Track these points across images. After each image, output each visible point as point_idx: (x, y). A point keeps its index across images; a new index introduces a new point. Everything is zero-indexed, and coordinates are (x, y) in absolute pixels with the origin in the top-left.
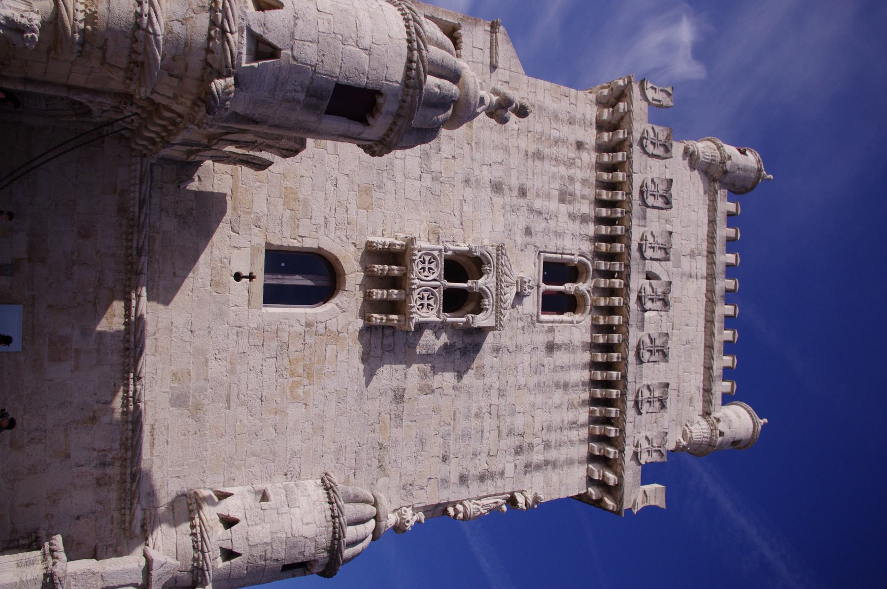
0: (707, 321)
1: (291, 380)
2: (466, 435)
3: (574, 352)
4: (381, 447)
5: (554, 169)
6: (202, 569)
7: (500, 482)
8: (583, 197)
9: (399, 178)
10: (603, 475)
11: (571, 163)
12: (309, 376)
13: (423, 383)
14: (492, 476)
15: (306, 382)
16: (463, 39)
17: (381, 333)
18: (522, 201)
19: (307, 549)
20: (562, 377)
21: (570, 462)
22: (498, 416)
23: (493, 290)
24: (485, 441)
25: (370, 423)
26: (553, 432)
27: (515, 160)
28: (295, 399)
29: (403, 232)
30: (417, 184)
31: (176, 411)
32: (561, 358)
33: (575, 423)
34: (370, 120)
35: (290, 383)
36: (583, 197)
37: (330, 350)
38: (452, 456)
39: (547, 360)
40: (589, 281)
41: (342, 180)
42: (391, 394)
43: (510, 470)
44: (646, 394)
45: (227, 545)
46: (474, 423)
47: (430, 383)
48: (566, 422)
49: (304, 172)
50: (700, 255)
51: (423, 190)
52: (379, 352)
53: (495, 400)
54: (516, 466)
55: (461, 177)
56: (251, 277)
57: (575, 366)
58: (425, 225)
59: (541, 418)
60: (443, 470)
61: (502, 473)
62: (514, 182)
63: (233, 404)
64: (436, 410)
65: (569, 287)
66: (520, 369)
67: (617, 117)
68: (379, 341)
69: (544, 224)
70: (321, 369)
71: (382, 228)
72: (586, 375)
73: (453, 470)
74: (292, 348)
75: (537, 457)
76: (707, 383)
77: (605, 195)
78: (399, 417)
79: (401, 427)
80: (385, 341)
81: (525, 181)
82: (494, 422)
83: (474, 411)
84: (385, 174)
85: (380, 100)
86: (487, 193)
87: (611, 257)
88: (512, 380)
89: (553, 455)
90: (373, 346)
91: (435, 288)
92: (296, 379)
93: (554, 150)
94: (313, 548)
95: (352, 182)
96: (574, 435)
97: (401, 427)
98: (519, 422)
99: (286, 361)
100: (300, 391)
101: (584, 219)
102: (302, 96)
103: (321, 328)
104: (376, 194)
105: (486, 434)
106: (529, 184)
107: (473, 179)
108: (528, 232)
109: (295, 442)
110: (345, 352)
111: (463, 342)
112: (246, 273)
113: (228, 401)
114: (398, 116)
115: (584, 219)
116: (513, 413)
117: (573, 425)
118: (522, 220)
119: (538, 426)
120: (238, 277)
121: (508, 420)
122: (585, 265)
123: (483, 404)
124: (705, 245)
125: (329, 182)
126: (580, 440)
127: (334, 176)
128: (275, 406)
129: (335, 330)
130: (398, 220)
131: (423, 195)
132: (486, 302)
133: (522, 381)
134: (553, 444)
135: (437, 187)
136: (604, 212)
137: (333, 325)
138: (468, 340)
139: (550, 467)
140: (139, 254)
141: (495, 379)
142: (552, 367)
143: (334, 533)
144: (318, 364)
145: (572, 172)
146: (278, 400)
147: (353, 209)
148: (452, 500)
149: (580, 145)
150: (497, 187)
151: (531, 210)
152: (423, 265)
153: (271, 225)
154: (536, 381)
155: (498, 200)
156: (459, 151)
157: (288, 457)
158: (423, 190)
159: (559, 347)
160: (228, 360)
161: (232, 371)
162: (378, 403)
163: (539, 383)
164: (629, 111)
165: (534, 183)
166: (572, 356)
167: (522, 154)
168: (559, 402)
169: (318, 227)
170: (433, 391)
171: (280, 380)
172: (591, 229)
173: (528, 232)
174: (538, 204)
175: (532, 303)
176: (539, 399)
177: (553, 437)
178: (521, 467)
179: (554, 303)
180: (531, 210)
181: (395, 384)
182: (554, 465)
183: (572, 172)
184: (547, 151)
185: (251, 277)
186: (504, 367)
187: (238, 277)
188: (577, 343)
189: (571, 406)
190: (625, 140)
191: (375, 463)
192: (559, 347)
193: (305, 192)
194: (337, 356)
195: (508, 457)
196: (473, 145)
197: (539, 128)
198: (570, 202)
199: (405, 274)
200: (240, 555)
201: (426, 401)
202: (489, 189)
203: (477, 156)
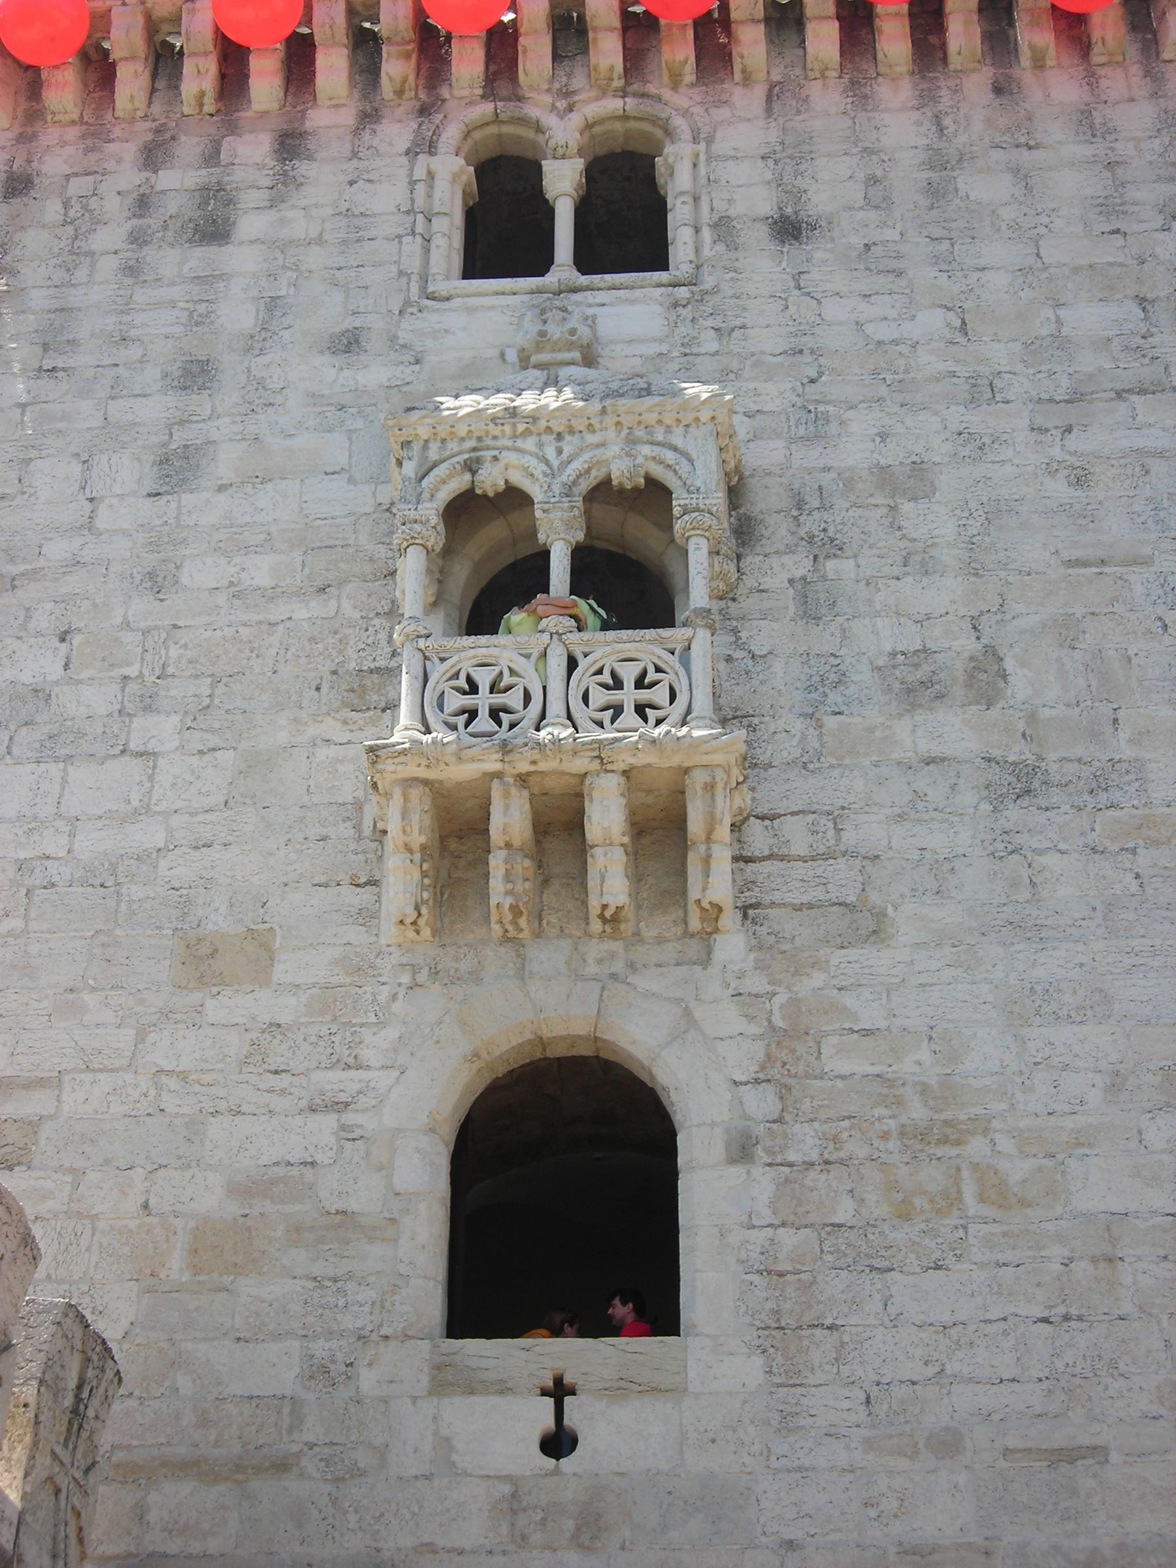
1: (973, 1207)
8: (212, 157)
9: (151, 835)
12: (951, 1134)
13: (959, 691)
15: (977, 1147)
17: (767, 867)
25: (1134, 886)
26: (1132, 194)
29: (359, 806)
30: (168, 769)
35: (990, 1212)
36: (212, 157)
37: (843, 1061)
40: (533, 112)
42: (1013, 813)
48: (1084, 151)
49: (131, 1205)
51: (196, 740)
55: (141, 607)
56: (559, 1391)
58: (331, 727)
62: (155, 409)
63: (1085, 1440)
64: (1066, 630)
65: (562, 182)
66: (884, 332)
70: (924, 1090)
71: (347, 891)
72: (896, 93)
74: (844, 1212)
80: (799, 847)
81: (152, 374)
83: (1058, 488)
86: (201, 507)
88: (929, 362)
90: (814, 894)
91: (572, 664)
92: (969, 1190)
95: (166, 1014)
99: (900, 1235)
100: (1017, 1170)
101: (290, 144)
103: (761, 1104)
108: (348, 344)
110: (849, 1000)
111: (790, 550)
112: (543, 1414)
113: (1069, 1455)
115: (290, 144)
116: (1060, 342)
118: (301, 370)
119: (1108, 252)
125: (169, 1103)
126: (1154, 95)
127: (145, 1083)
128: (1082, 1268)
130: (314, 832)
131: (214, 741)
133: (933, 322)
137: (742, 1058)
142: (872, 215)
144: (899, 1102)
145: (113, 206)
146: (1057, 1252)
150: (176, 468)
152: (483, 713)
153: (349, 1322)
154: (931, 272)
155: (226, 461)
156: (42, 621)
158: (196, 740)
160: (903, 1463)
161: (947, 1444)
162: (1051, 860)
163: (936, 259)
170: (991, 651)
173: (348, 344)
174: (237, 314)
175: (627, 312)
179: (627, 224)
181: (968, 797)
184: (39, 299)
185: (559, 1391)
186: (883, 391)
187: (558, 1443)
188: (774, 135)
194: (867, 1033)
196: (14, 570)
198: (230, 202)
199: (523, 779)
202: (187, 498)
203: (58, 550)
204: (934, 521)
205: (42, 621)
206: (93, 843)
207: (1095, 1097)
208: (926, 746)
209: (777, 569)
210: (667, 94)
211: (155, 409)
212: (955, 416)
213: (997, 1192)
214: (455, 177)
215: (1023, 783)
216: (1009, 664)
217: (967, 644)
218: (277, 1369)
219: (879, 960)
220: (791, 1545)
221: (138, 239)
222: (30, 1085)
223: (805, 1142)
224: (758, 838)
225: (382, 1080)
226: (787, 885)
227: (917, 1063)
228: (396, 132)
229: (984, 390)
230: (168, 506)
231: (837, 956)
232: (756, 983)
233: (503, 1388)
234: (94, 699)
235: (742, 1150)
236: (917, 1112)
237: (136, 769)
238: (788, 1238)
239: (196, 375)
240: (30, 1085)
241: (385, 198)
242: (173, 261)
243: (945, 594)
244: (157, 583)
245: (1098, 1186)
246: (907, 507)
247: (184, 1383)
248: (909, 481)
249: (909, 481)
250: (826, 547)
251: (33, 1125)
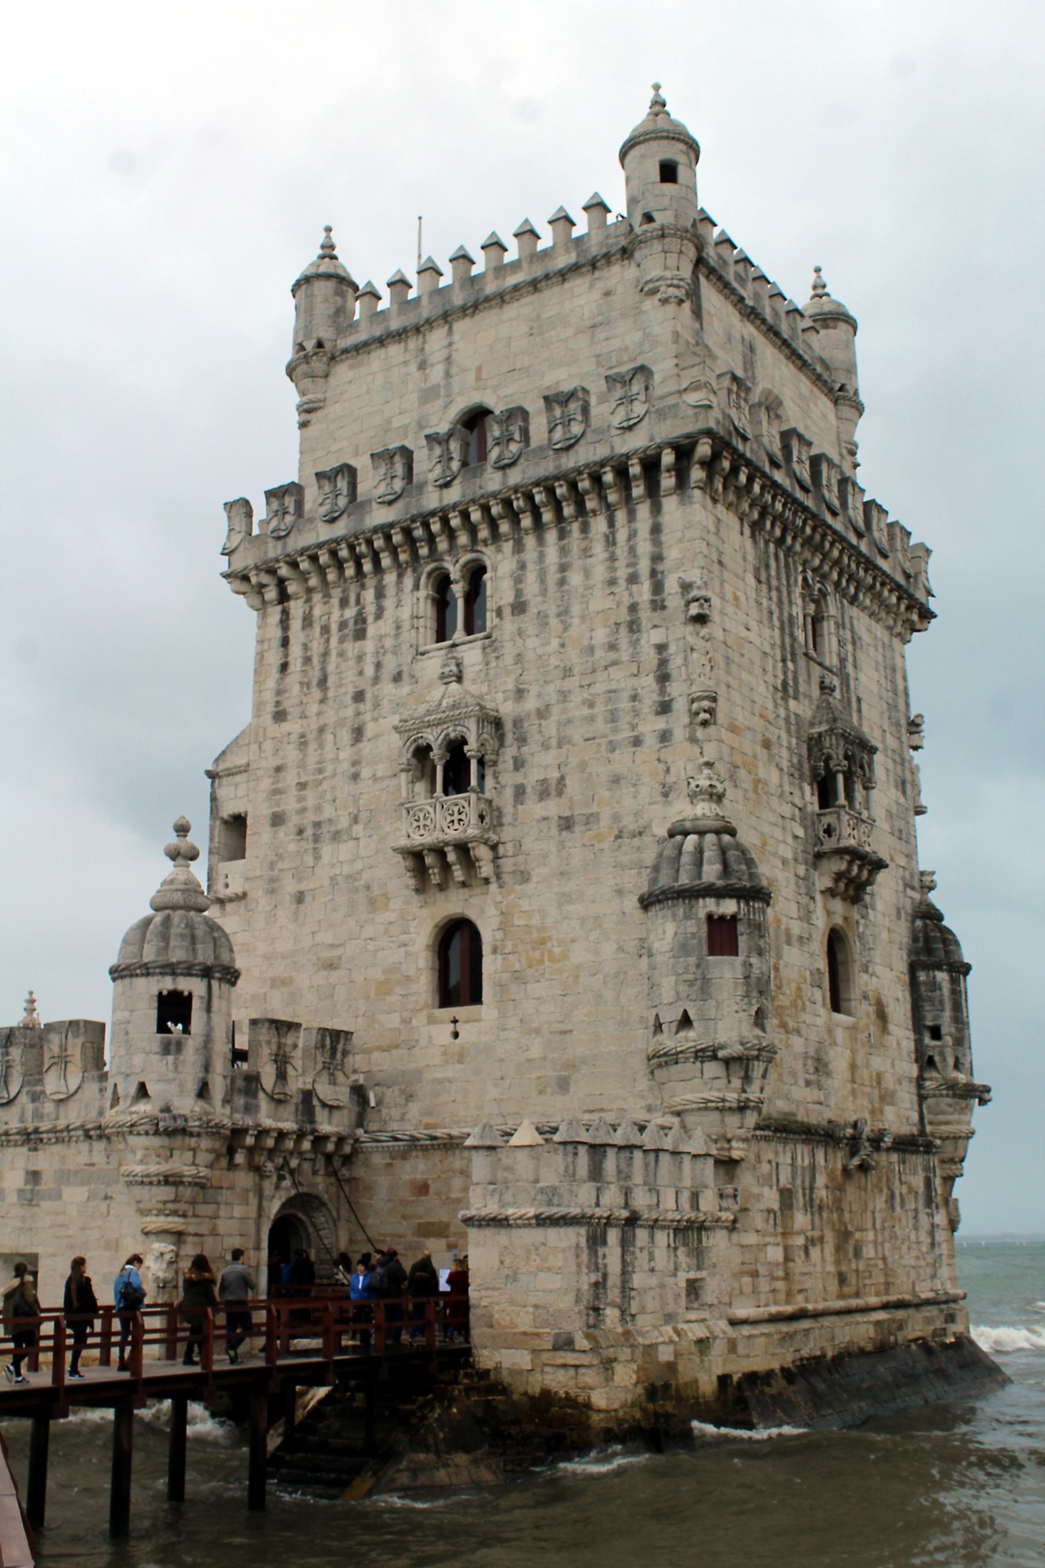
0: (503, 301)
1: (547, 963)
2: (613, 717)
3: (522, 566)
4: (619, 837)
5: (334, 653)
6: (696, 1052)
7: (672, 649)
9: (359, 865)
10: (668, 471)
11: (326, 630)
12: (543, 942)
13: (554, 793)
14: (663, 663)
15: (549, 944)
16: (231, 812)
18: (368, 696)
19: (689, 930)
20: (552, 577)
21: (656, 530)
22: (594, 671)
23: (440, 728)
24: (622, 685)
27: (330, 716)
28: (565, 956)
30: (362, 842)
31: (572, 1088)
32: (531, 585)
33: (607, 536)
34: (186, 993)
37: (519, 921)
38: (635, 733)
39: (533, 610)
40: (446, 565)
41: (365, 934)
42: (564, 833)
43: (657, 636)
44: (558, 434)
45: (674, 1026)
46: (600, 709)
47: (553, 784)
50: (423, 349)
52: (521, 858)
53: (572, 683)
54: (655, 626)
57: (542, 556)
59: (600, 601)
60: (651, 742)
61: (661, 648)
63: (568, 1028)
66: (540, 651)
67: (265, 579)
68: (510, 861)
69: (389, 656)
72: (551, 536)
73: (651, 725)
74: (517, 967)
75: (644, 592)
76: (584, 270)
77: (350, 571)
78: (591, 819)
79: (598, 814)
80: (511, 853)
82: (601, 676)
83: (586, 711)
84: (356, 884)
85: (165, 993)
87: (411, 541)
88: (554, 661)
89: (644, 567)
93: (315, 660)
94: (689, 923)
96: (622, 535)
97: (598, 814)
98: (601, 636)
99: (529, 972)
100: (557, 951)
101: (380, 594)
102: (170, 1058)
103: (499, 935)
104: (376, 891)
105: (614, 685)
106: (351, 690)
107: (353, 770)
108: (397, 678)
109: (608, 948)
110: (521, 902)
112: (451, 1027)
113: (564, 1032)
114: (174, 974)
115: (380, 594)
117: (610, 541)
119: (609, 603)
120: (456, 1035)
121: (599, 653)
122: (430, 574)
123: (579, 699)
124: (413, 343)
125: (369, 947)
129: (499, 919)
132: (452, 735)
133: (555, 643)
134: (631, 570)
135: (364, 816)
136: (367, 566)
137: (495, 922)
138: (509, 738)
139: (660, 567)
140: (435, 1138)
141: (552, 686)
143: (673, 899)
144: (531, 933)
145: (334, 627)
146: (565, 975)
147: (390, 916)
148: (686, 720)
149: (308, 621)
150: (358, 733)
151: (376, 680)
153: (410, 1006)
156: (329, 796)
157: (622, 955)
159: (519, 593)
161: (537, 1031)
162: (572, 851)
164: (256, 567)
165: (351, 682)
166: (530, 567)
167: (324, 707)
168: (582, 573)
169: (408, 954)
171: (547, 976)
172: (390, 578)
173: (397, 678)
174: (369, 671)
175: (471, 654)
176: (576, 609)
177: (622, 573)
178: (657, 617)
180: (376, 680)
181: (554, 831)
182: (657, 558)
183: (334, 627)
185: (455, 1021)
189: (586, 553)
190: (287, 563)
191: (636, 842)
192: (519, 593)
193: (378, 974)
195: (643, 642)
196: (320, 777)
197: (296, 689)
198: (364, 621)
200: (685, 1012)
201: (573, 787)
202: (361, 745)
204: (550, 727)
205: (329, 796)
206: (346, 869)
207: (578, 927)
208: (545, 814)
209: (509, 752)
210: (484, 549)
211: (349, 712)
212: (558, 684)
213: (552, 959)
214: (426, 598)
215: (567, 824)
216: (567, 782)
217: (556, 775)
218: (393, 1021)
219: (529, 888)
220: (502, 1060)
221: (342, 640)
222: (339, 945)
223: (509, 948)
224: (501, 850)
225: (414, 936)
226: (507, 865)
227: (535, 921)
228: (408, 581)
229: (567, 672)
230: (355, 749)
231: (517, 888)
232: (499, 898)
233: (442, 1022)
234: (344, 822)
235: (495, 951)
236: (535, 935)
237: (352, 843)
238: (505, 976)
239: (359, 697)
240: (339, 945)
241: (405, 613)
242: (352, 648)
243: (550, 758)
244: (355, 777)
245: (579, 955)
246: (544, 723)
247: (376, 1026)
248: (542, 714)
249: (542, 714)
250: (522, 740)
251: (340, 958)
